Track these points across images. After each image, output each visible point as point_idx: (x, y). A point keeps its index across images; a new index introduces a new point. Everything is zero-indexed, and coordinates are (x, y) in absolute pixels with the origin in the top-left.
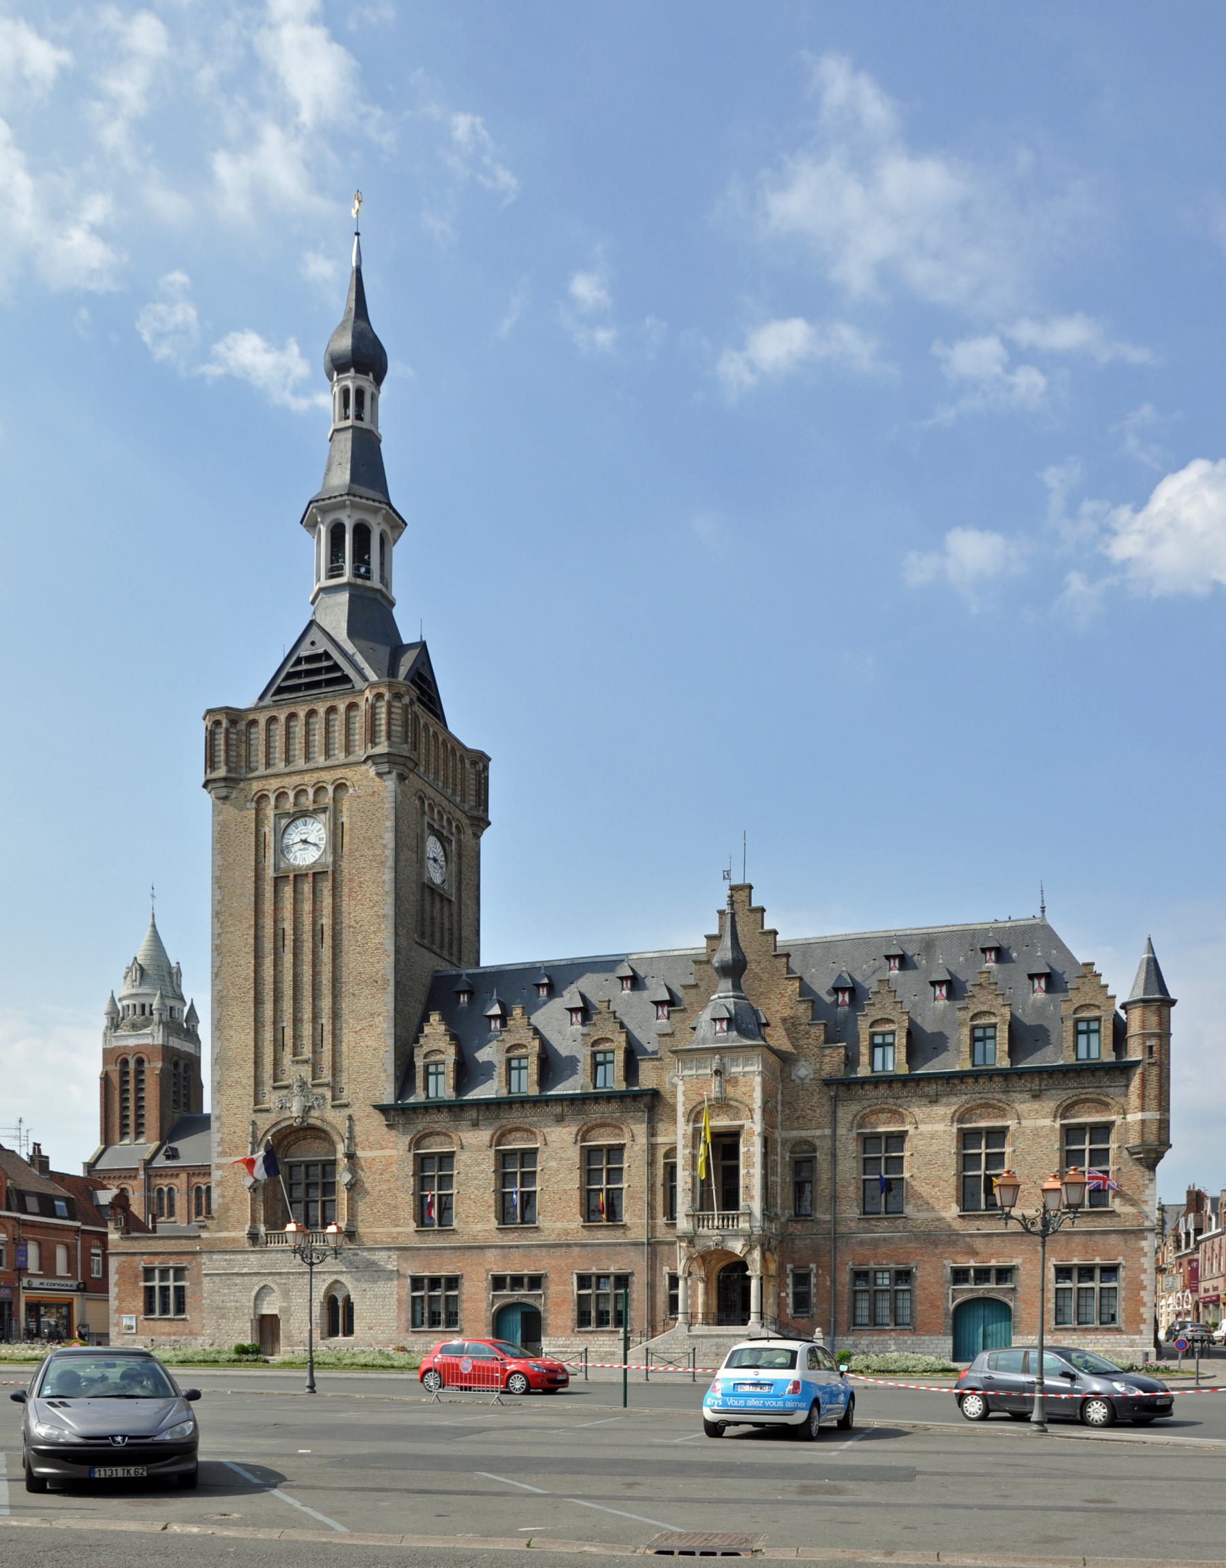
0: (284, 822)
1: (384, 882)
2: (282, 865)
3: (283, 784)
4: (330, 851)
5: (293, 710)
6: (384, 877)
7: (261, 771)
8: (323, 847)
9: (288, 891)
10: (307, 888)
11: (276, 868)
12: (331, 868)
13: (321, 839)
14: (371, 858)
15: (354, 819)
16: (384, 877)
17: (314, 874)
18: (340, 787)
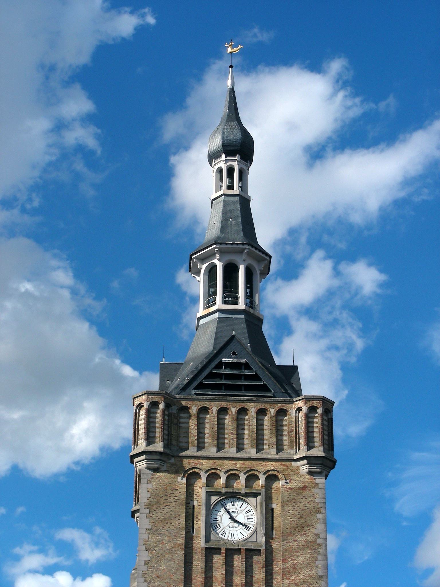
0: (214, 499)
1: (317, 566)
2: (212, 538)
3: (214, 466)
4: (262, 531)
5: (224, 404)
6: (317, 563)
7: (192, 451)
8: (253, 528)
9: (219, 561)
10: (238, 561)
11: (208, 540)
12: (264, 548)
13: (250, 520)
14: (304, 544)
15: (286, 507)
16: (317, 563)
17: (247, 550)
18: (272, 478)
